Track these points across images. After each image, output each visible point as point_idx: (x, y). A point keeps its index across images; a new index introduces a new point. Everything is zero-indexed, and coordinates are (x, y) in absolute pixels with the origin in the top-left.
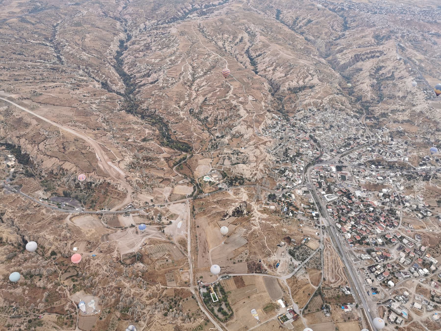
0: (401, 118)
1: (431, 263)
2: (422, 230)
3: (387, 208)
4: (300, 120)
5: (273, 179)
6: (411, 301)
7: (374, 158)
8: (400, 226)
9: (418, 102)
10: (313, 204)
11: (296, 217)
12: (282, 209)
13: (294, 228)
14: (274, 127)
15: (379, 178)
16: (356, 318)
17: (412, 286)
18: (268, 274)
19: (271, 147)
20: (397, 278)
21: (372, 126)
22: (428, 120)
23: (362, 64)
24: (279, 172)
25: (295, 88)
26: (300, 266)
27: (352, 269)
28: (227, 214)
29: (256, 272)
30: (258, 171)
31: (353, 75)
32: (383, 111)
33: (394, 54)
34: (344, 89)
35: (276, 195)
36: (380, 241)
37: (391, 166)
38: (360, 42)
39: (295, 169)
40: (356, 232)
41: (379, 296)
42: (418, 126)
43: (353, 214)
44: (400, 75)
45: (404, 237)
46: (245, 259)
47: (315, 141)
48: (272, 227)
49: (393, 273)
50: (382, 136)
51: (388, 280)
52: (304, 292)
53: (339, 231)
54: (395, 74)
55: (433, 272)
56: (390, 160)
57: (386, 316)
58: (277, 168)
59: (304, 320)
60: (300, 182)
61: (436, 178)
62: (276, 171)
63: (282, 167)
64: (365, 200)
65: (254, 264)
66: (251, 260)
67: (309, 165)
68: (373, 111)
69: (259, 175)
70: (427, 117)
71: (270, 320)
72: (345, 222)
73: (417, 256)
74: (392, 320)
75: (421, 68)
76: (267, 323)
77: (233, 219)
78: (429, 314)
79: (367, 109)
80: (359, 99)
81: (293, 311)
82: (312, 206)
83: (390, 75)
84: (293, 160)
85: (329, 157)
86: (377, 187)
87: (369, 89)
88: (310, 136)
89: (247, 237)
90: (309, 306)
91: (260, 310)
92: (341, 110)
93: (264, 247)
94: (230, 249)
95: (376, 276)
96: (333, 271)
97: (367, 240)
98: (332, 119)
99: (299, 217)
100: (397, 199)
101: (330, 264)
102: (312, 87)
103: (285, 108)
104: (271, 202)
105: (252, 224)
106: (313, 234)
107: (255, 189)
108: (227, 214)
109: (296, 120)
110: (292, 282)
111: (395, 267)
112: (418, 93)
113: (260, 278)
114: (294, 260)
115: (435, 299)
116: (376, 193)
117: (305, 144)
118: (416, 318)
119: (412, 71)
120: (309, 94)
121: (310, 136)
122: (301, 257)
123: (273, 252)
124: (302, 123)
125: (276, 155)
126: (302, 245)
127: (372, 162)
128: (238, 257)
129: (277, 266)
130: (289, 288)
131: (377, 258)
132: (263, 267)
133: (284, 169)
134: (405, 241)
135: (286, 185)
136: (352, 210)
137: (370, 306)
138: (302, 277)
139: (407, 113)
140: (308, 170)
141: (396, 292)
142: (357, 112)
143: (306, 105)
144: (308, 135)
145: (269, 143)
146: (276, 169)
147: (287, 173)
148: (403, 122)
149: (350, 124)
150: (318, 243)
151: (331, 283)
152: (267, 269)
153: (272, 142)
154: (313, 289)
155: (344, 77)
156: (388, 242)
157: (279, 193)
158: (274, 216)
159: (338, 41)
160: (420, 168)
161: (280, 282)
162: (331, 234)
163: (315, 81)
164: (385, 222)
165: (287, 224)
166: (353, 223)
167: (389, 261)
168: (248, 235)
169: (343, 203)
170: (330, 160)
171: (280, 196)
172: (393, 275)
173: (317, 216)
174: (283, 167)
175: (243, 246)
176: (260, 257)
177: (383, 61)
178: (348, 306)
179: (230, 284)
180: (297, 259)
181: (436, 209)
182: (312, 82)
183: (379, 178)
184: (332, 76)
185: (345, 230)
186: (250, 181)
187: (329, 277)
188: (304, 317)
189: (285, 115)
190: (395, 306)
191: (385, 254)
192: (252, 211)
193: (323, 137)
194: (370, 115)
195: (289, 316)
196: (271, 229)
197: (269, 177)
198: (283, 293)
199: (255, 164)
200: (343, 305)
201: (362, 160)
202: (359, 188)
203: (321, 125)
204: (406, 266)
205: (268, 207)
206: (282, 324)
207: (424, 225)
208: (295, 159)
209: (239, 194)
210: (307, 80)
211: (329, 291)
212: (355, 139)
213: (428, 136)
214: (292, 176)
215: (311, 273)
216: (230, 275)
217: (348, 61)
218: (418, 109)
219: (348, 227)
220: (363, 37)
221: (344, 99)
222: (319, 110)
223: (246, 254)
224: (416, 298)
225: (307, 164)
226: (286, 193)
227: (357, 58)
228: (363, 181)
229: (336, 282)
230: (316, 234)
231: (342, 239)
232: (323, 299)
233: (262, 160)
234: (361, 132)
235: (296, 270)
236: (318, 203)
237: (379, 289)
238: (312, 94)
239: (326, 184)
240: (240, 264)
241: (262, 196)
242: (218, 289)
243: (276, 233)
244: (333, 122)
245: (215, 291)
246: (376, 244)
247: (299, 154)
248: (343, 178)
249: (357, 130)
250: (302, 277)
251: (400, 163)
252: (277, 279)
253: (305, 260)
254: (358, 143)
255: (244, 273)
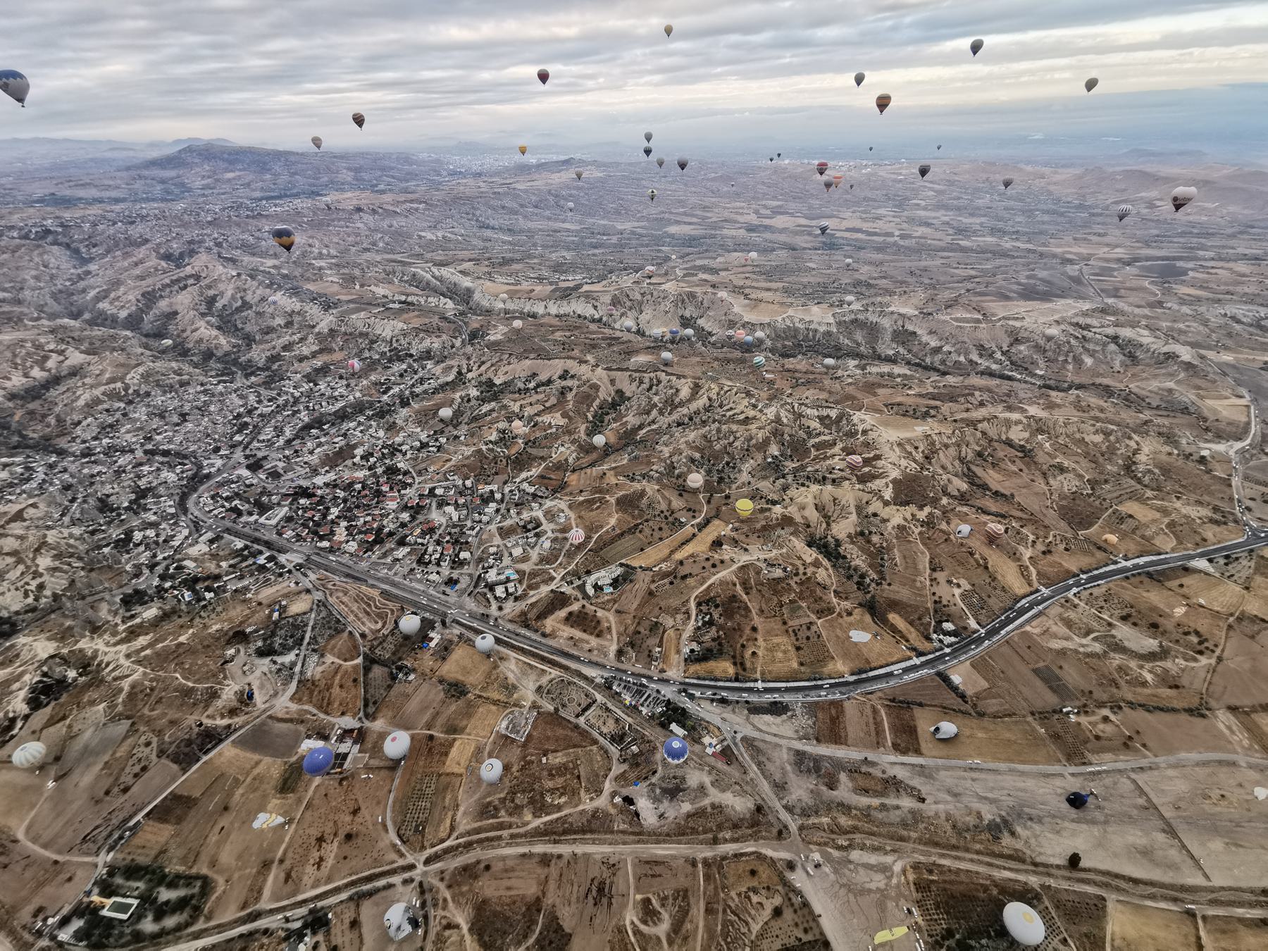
0: (306, 351)
1: (492, 492)
2: (449, 464)
3: (380, 470)
4: (95, 438)
5: (110, 567)
6: (506, 554)
7: (306, 419)
8: (418, 480)
9: (316, 320)
10: (246, 547)
11: (225, 592)
12: (179, 601)
13: (237, 612)
14: (28, 480)
15: (336, 440)
16: (456, 639)
17: (492, 536)
18: (241, 727)
19: (48, 516)
20: (467, 543)
21: (264, 383)
22: (350, 336)
23: (171, 305)
24: (115, 547)
25: (27, 391)
26: (301, 657)
27: (394, 584)
28: (13, 721)
29: (206, 753)
30: (41, 575)
31: (165, 326)
32: (268, 354)
33: (219, 270)
34: (163, 352)
35: (142, 587)
36: (405, 516)
37: (342, 416)
38: (138, 271)
39: (153, 518)
40: (360, 532)
41: (462, 585)
42: (341, 349)
43: (335, 512)
44: (257, 298)
45: (434, 488)
46: (154, 757)
47: (166, 453)
48: (181, 644)
49: (457, 542)
50: (295, 388)
51: (457, 555)
52: (341, 686)
53: (331, 550)
54: (248, 298)
55: (502, 500)
56: (332, 409)
57: (492, 600)
58: (104, 543)
59: (378, 725)
60: (186, 532)
61: (417, 396)
62: (106, 550)
63: (116, 533)
64: (339, 482)
65: (189, 742)
66: (171, 743)
67: (184, 498)
68: (250, 361)
69: (56, 584)
70: (345, 334)
71: (310, 793)
72: (332, 533)
73: (469, 498)
74: (504, 596)
75: (285, 276)
76: (307, 807)
77: (45, 713)
78: (537, 549)
79: (235, 362)
80: (208, 355)
81: (347, 733)
82: (246, 553)
83: (239, 303)
84: (137, 506)
85: (219, 463)
86: (343, 454)
87: (215, 332)
88: (146, 452)
89: (120, 714)
90: (369, 696)
91: (275, 802)
92: (182, 384)
93: (188, 692)
94: (86, 778)
95: (438, 564)
96: (368, 614)
97: (386, 530)
98: (176, 403)
99: (231, 587)
100: (386, 451)
101: (355, 608)
102: (75, 372)
103: (32, 435)
104: (138, 609)
105: (115, 679)
106: (286, 591)
107: (65, 616)
108: (13, 721)
109: (84, 442)
110: (307, 692)
111: (453, 531)
112: (307, 308)
113: (226, 752)
114: (280, 659)
115: (529, 527)
116: (349, 462)
117: (146, 468)
118: (526, 567)
119: (272, 284)
120: (80, 384)
121: (146, 452)
122: (290, 642)
123: (219, 683)
124: (105, 441)
125: (73, 523)
126: (276, 623)
127: (307, 427)
128: (127, 770)
129: (251, 696)
130: (306, 707)
131: (419, 541)
132: (215, 729)
133: (126, 534)
134: (439, 492)
135: (155, 556)
136: (328, 509)
137: (461, 607)
138: (320, 669)
139: (311, 339)
140: (190, 504)
141: (480, 560)
142: (222, 375)
143: (87, 405)
144: (139, 454)
145: (31, 511)
146: (100, 547)
147: (138, 536)
148: (314, 355)
149: (221, 394)
150: (308, 597)
151: (379, 631)
152: (230, 721)
153: (42, 506)
154: (355, 667)
155: (147, 336)
156: (416, 510)
157: (147, 581)
158: (167, 626)
159: (82, 284)
160: (385, 397)
161: (280, 715)
162: (319, 566)
163: (75, 357)
164: (391, 489)
165: (213, 616)
166: (344, 524)
167: (439, 532)
168: (120, 708)
169: (305, 509)
170: (224, 465)
171: (155, 583)
172: (459, 542)
173: (271, 559)
174: (119, 531)
175: (126, 738)
176: (191, 719)
177: (209, 287)
178: (432, 635)
179: (149, 836)
180: (286, 649)
181: (446, 430)
182: (67, 363)
183: (336, 440)
184: (113, 338)
185: (341, 543)
186: (33, 610)
187: (369, 626)
188: (374, 719)
189: (45, 445)
190: (492, 576)
191: (425, 527)
192: (95, 656)
193: (178, 439)
194: (249, 369)
195: (343, 748)
196: (181, 650)
197: (92, 570)
198: (302, 728)
199: (21, 568)
200: (423, 642)
201: (288, 433)
202: (315, 472)
203: (156, 422)
204: (466, 519)
205: (138, 620)
206: (341, 773)
207: (447, 456)
208: (139, 506)
209: (17, 656)
210: (51, 364)
211: (385, 645)
212: (250, 412)
213: (367, 354)
214: (157, 535)
215: (334, 647)
216: (131, 823)
217: (134, 308)
218: (323, 327)
219: (341, 533)
220: (136, 264)
221: (174, 364)
222: (130, 402)
223: (148, 744)
224: (509, 545)
225: (177, 498)
226: (167, 568)
227: (150, 298)
228: (314, 459)
229: (385, 624)
230: (292, 585)
231: (345, 559)
232: (383, 663)
233: (37, 550)
234: (252, 398)
235: (297, 669)
236: (256, 541)
237: (455, 576)
238: (87, 380)
239: (249, 502)
240: (147, 775)
241: (104, 612)
242: (119, 880)
243: (200, 647)
244: (182, 406)
245: (109, 896)
246: (403, 525)
247: (142, 494)
248: (275, 475)
249: (241, 397)
250: (320, 669)
251: (351, 406)
252: (270, 717)
253: (303, 638)
254: (260, 415)
255: (174, 780)
